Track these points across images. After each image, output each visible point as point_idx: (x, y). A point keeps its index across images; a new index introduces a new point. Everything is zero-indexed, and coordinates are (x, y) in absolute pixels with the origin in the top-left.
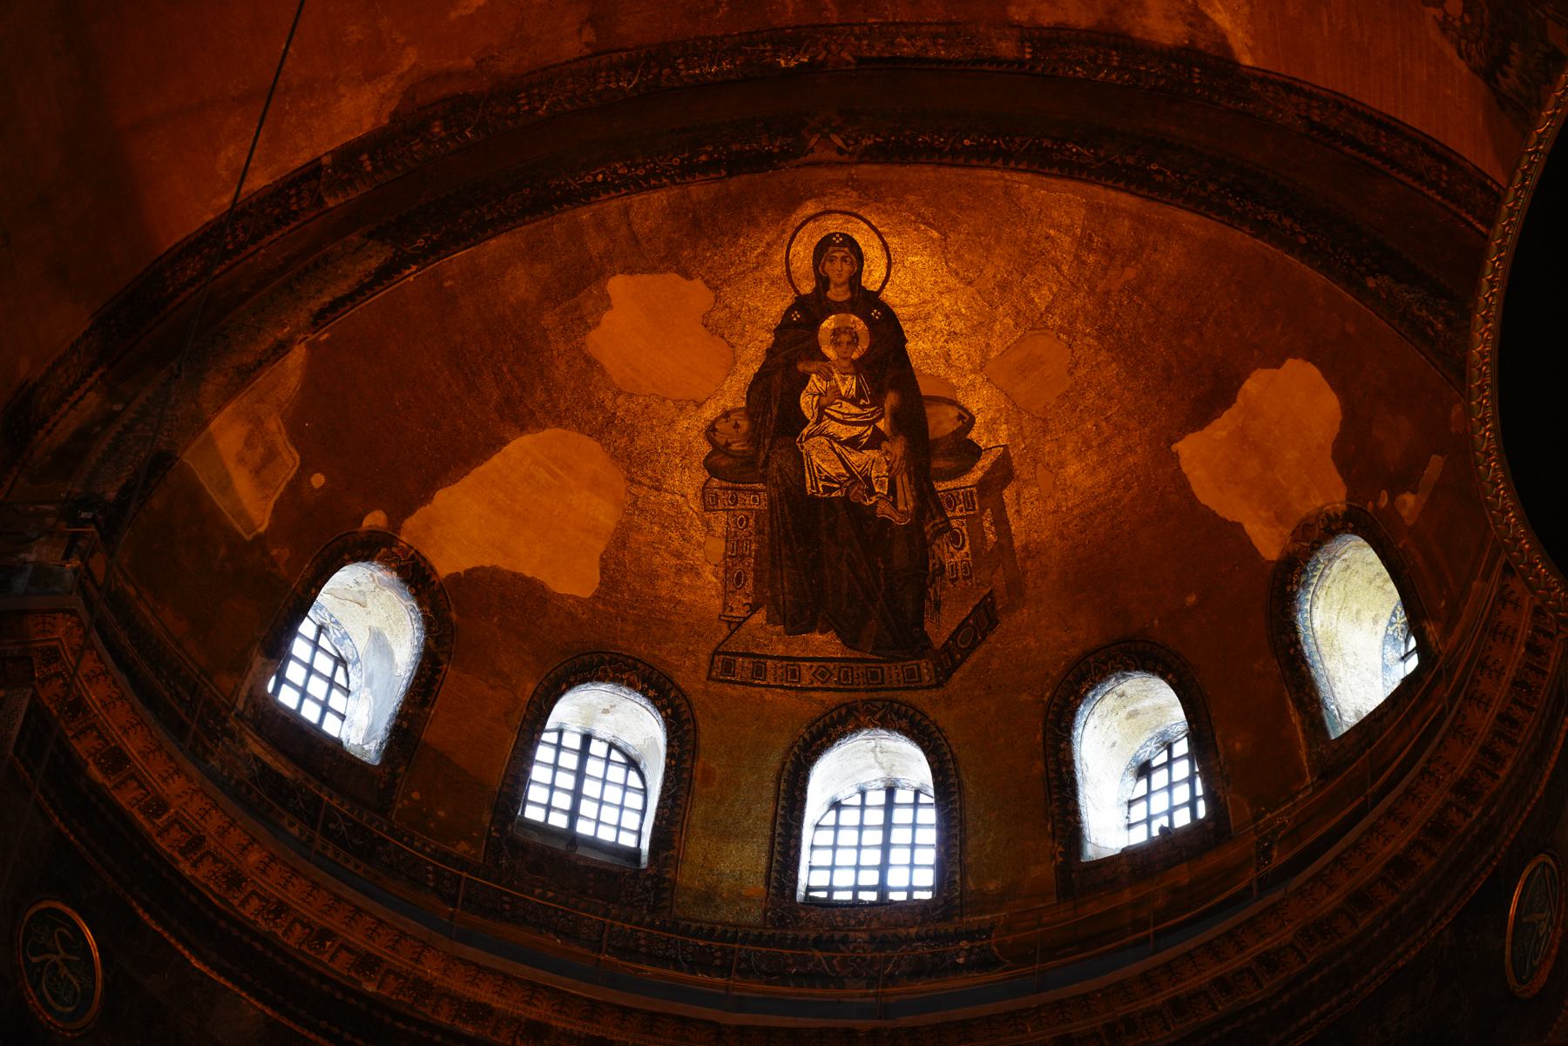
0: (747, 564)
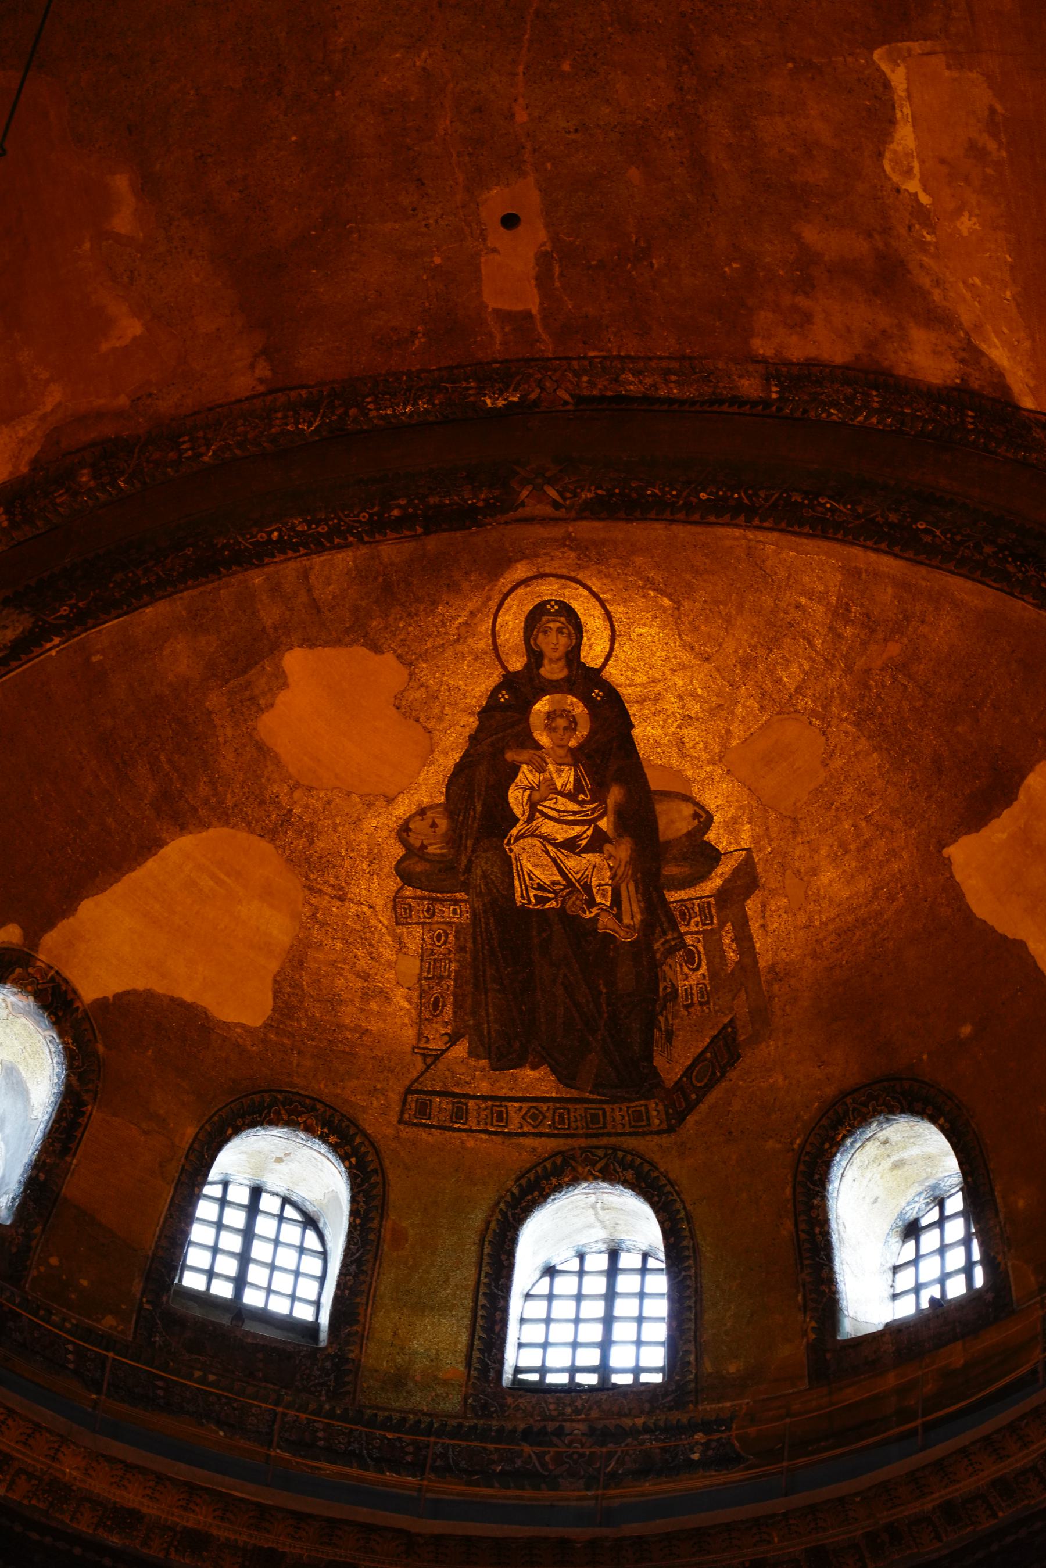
0: (445, 987)
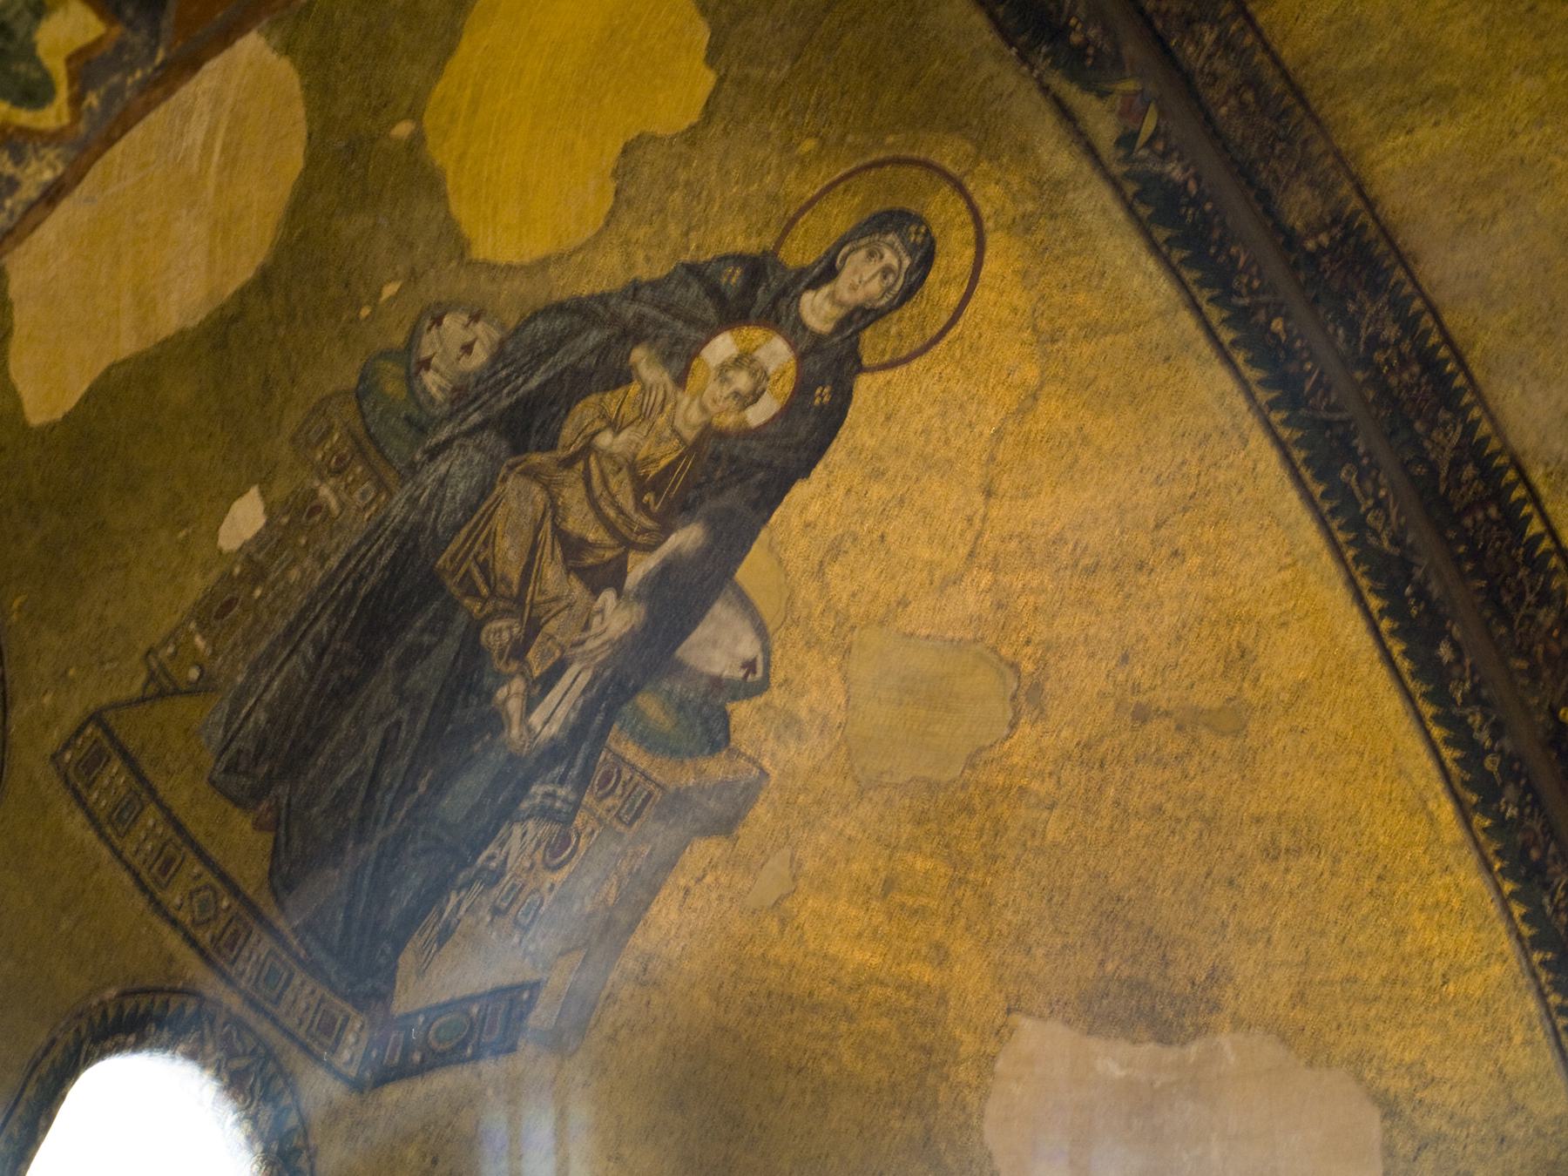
0: (258, 593)
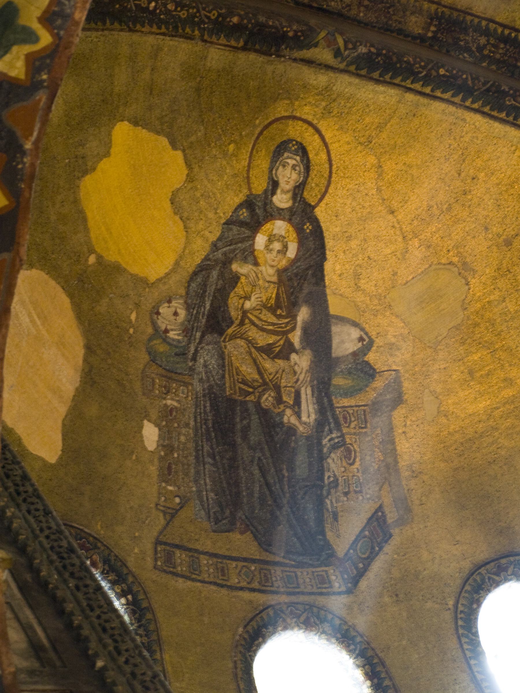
0: (176, 455)
